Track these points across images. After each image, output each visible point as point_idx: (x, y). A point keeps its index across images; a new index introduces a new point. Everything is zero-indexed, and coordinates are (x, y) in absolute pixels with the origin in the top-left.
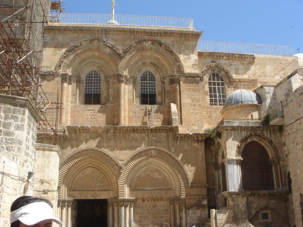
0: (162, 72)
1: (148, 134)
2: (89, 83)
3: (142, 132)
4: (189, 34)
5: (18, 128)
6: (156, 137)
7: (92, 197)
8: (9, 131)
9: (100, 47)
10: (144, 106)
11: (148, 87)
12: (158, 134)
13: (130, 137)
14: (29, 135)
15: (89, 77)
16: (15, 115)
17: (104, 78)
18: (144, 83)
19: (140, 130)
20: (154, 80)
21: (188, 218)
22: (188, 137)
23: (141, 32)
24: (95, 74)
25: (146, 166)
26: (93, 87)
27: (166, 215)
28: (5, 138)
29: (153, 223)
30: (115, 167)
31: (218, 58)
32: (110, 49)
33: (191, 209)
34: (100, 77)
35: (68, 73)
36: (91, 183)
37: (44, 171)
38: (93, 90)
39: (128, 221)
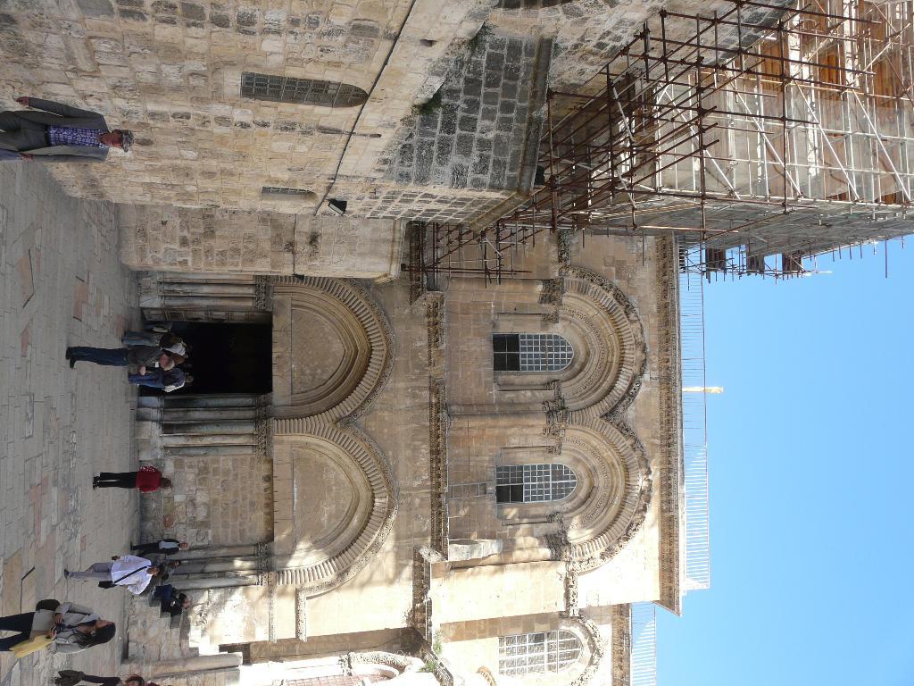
1: (427, 487)
2: (543, 343)
6: (421, 506)
7: (278, 357)
9: (629, 367)
10: (492, 473)
12: (428, 511)
13: (420, 442)
14: (439, 201)
15: (557, 343)
17: (556, 377)
18: (547, 473)
24: (563, 356)
25: (351, 482)
27: (230, 536)
28: (433, 143)
29: (211, 502)
30: (349, 409)
31: (617, 656)
32: (624, 390)
34: (557, 368)
35: (567, 293)
36: (310, 353)
39: (218, 440)
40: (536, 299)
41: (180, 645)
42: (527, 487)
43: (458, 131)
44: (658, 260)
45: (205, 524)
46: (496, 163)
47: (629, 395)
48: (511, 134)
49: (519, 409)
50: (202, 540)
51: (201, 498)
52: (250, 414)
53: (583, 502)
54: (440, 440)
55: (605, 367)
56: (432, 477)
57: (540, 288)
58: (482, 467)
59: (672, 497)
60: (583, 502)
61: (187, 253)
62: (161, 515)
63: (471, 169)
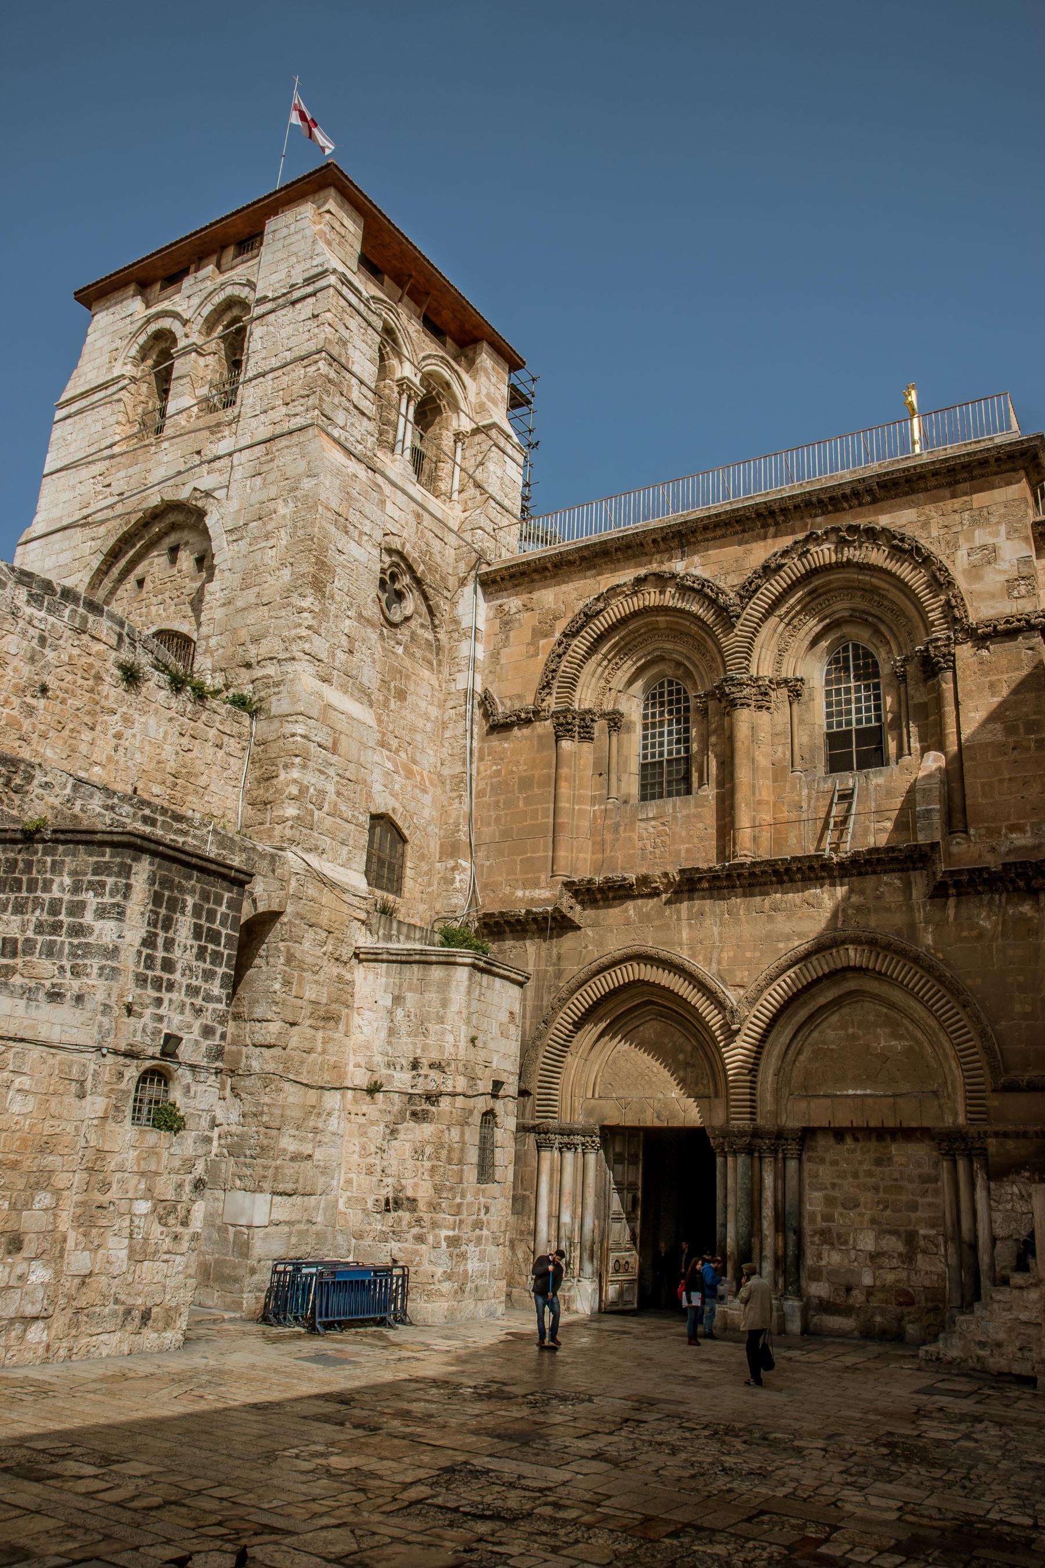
0: (896, 637)
3: (810, 879)
4: (983, 463)
5: (101, 913)
6: (862, 892)
8: (81, 925)
11: (853, 706)
12: (870, 881)
14: (166, 928)
15: (653, 705)
16: (97, 878)
19: (799, 869)
20: (876, 675)
21: (998, 1217)
22: (984, 880)
23: (796, 507)
24: (670, 693)
26: (666, 738)
27: (929, 1200)
33: (1011, 1177)
34: (687, 700)
37: (425, 1034)
38: (666, 748)
39: (768, 1211)
40: (586, 746)
41: (1021, 1288)
42: (859, 721)
43: (62, 917)
44: (533, 581)
45: (910, 1238)
46: (98, 870)
47: (700, 590)
48: (68, 859)
49: (728, 752)
50: (937, 1246)
51: (867, 1242)
52: (730, 1159)
53: (877, 632)
54: (757, 870)
55: (676, 633)
56: (817, 878)
57: (566, 745)
58: (817, 799)
59: (848, 491)
60: (877, 632)
61: (436, 1236)
62: (893, 1308)
63: (100, 900)
